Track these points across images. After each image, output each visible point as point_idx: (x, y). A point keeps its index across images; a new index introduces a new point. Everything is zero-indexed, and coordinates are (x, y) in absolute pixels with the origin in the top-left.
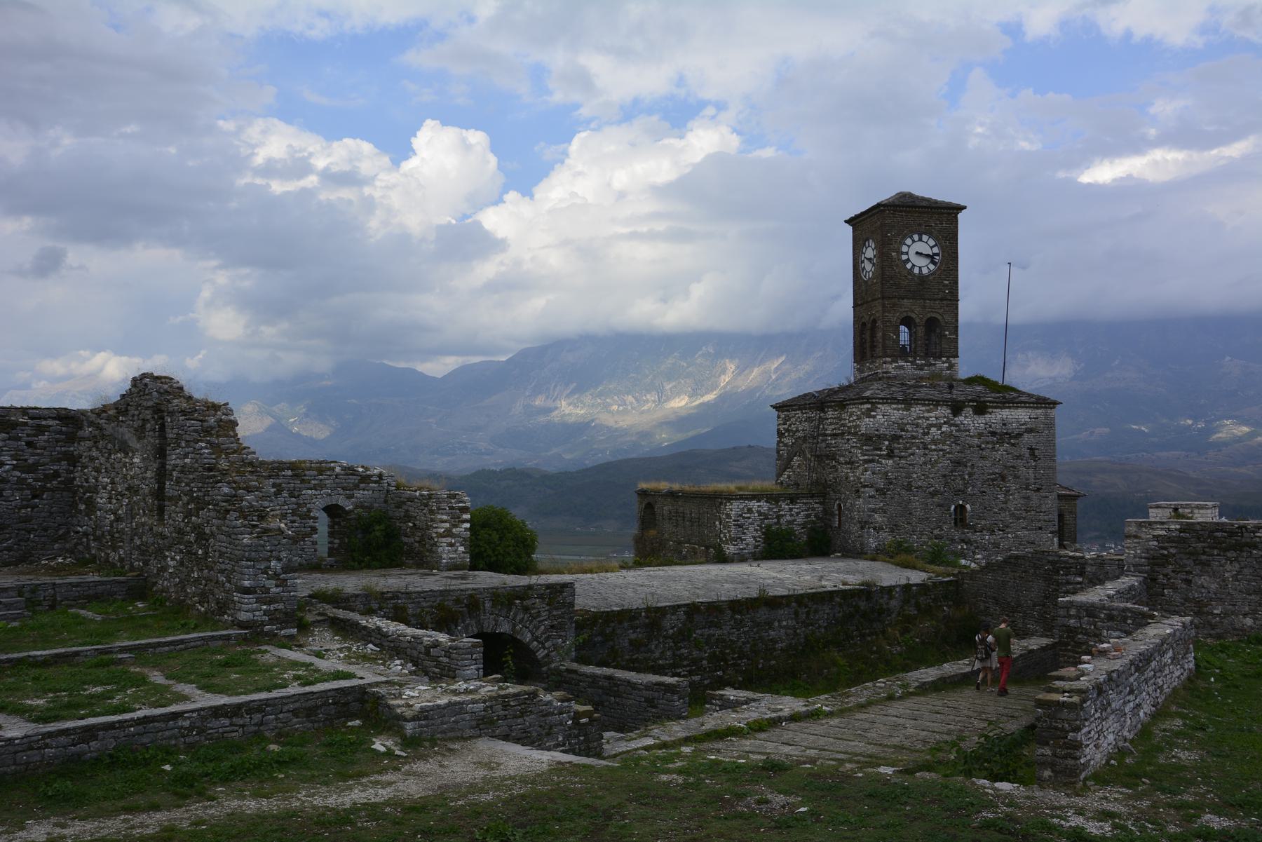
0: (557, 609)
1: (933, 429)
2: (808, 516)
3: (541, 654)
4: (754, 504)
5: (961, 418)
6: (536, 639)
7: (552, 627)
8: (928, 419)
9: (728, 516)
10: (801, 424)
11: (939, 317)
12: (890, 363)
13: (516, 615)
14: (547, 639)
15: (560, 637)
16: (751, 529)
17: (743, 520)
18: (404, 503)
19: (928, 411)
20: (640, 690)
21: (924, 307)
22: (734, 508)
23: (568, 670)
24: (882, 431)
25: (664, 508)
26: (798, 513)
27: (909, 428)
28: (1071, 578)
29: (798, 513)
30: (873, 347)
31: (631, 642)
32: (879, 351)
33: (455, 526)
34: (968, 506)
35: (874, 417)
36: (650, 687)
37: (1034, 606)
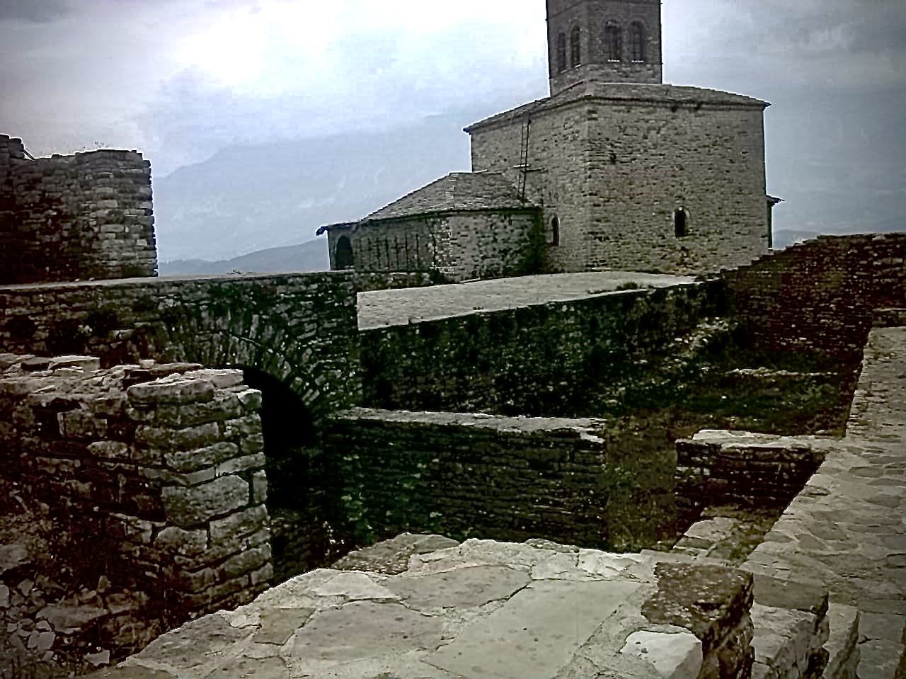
0: (329, 318)
1: (653, 132)
2: (521, 235)
3: (311, 396)
4: (471, 221)
5: (679, 120)
6: (298, 371)
7: (325, 350)
8: (647, 121)
9: (445, 235)
10: (506, 144)
11: (643, 22)
12: (597, 70)
13: (260, 330)
14: (317, 371)
15: (339, 366)
16: (470, 247)
17: (461, 242)
18: (39, 180)
19: (649, 113)
20: (519, 447)
21: (628, 10)
22: (452, 223)
23: (361, 422)
24: (606, 134)
25: (359, 242)
26: (512, 231)
27: (629, 131)
28: (887, 261)
29: (512, 231)
30: (576, 56)
31: (406, 370)
32: (584, 58)
33: (130, 205)
34: (687, 213)
35: (595, 119)
36: (537, 439)
37: (832, 296)
